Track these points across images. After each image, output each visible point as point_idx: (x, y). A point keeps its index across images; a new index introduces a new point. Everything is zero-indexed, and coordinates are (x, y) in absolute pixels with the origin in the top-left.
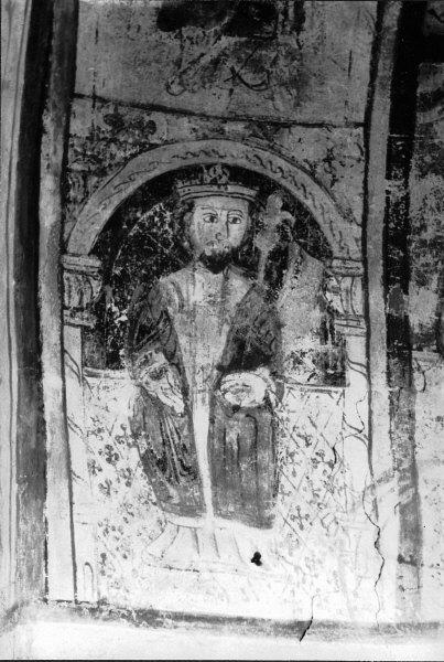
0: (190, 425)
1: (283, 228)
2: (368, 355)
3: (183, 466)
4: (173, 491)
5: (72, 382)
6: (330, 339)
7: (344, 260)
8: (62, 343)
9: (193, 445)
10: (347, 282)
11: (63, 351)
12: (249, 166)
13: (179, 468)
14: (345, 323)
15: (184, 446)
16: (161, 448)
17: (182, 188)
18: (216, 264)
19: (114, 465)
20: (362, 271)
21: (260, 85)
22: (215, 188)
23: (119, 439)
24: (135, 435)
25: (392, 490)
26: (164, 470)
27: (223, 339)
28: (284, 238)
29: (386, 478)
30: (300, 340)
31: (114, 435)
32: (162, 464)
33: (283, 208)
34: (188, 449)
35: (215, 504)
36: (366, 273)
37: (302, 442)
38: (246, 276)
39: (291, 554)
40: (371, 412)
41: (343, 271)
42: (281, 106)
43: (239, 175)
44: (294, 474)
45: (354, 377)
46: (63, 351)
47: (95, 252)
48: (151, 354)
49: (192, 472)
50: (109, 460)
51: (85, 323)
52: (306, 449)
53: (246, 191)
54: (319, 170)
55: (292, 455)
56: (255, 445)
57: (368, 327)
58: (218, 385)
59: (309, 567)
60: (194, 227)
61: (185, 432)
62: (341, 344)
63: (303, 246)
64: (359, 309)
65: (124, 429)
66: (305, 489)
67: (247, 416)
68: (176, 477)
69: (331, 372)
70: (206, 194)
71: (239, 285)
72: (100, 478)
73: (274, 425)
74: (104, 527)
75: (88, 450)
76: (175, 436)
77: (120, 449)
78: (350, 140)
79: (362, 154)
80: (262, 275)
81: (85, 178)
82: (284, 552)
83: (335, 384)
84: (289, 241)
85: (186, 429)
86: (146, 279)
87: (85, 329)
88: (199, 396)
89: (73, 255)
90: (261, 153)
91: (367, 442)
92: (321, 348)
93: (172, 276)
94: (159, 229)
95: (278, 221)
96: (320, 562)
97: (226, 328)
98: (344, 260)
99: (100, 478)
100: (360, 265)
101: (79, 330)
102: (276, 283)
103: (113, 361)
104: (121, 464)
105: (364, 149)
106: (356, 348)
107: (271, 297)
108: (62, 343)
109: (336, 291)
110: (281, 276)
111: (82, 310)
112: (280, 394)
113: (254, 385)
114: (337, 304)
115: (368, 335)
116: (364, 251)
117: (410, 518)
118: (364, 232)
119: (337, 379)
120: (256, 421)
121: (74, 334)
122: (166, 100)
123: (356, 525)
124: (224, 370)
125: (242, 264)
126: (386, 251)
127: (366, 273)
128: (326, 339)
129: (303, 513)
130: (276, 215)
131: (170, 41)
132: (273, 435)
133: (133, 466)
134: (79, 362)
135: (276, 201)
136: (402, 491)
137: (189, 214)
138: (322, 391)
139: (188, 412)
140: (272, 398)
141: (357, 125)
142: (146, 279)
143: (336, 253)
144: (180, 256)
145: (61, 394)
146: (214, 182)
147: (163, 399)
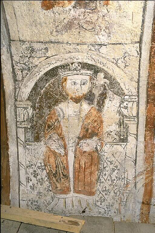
0: (67, 159)
1: (104, 85)
2: (137, 131)
3: (63, 175)
4: (58, 185)
5: (21, 149)
6: (122, 126)
7: (130, 96)
8: (17, 135)
9: (67, 166)
10: (130, 105)
11: (17, 138)
12: (90, 62)
13: (61, 175)
14: (129, 120)
15: (64, 167)
16: (55, 169)
17: (62, 73)
18: (77, 100)
19: (36, 178)
20: (137, 100)
21: (92, 29)
22: (75, 72)
23: (39, 168)
24: (45, 165)
25: (143, 178)
26: (55, 177)
27: (80, 127)
28: (105, 89)
29: (141, 173)
30: (110, 126)
31: (37, 166)
32: (55, 175)
33: (104, 78)
34: (66, 168)
35: (74, 188)
36: (138, 100)
37: (109, 163)
38: (89, 104)
39: (101, 204)
40: (136, 152)
41: (129, 100)
42: (103, 39)
43: (85, 66)
44: (105, 175)
45: (131, 139)
46: (17, 138)
47: (29, 99)
48: (52, 135)
49: (66, 177)
50: (34, 176)
51: (26, 126)
52: (110, 166)
53: (89, 72)
54: (119, 61)
55: (105, 168)
56: (91, 164)
57: (138, 121)
58: (78, 144)
59: (107, 208)
60: (67, 86)
61: (65, 162)
62: (127, 128)
63: (113, 92)
64: (135, 114)
65: (41, 164)
66: (109, 180)
67: (89, 154)
68: (60, 179)
69: (123, 138)
70: (72, 74)
71: (85, 107)
72: (31, 184)
73: (99, 158)
74: (31, 201)
75: (26, 173)
76: (61, 164)
77: (39, 171)
78: (133, 49)
79: (138, 54)
80: (96, 103)
81: (22, 72)
82: (99, 204)
83: (123, 142)
84: (107, 90)
85: (65, 160)
86: (50, 107)
87: (26, 128)
88: (71, 148)
89: (20, 101)
90: (94, 57)
91: (134, 162)
92: (118, 130)
93: (60, 105)
94: (53, 89)
95: (102, 83)
96: (112, 206)
97: (81, 124)
98: (130, 96)
99: (31, 184)
100: (136, 97)
101: (23, 129)
102: (101, 104)
103: (37, 139)
104: (39, 177)
105: (139, 52)
106: (132, 129)
107: (100, 110)
108: (17, 135)
109: (126, 108)
110: (103, 102)
111: (24, 121)
112: (102, 146)
113: (89, 145)
114: (125, 112)
115: (138, 124)
116: (138, 92)
117: (149, 188)
118: (138, 85)
119: (124, 140)
120: (92, 157)
121: (21, 131)
122: (53, 39)
123: (127, 192)
124: (80, 139)
125: (88, 99)
126: (148, 91)
127: (138, 100)
128: (121, 125)
129: (107, 188)
130: (101, 79)
131: (49, 13)
132: (98, 161)
133: (44, 177)
134: (24, 141)
135: (101, 75)
136: (146, 179)
137: (65, 82)
138: (118, 145)
139: (66, 154)
140: (99, 148)
141: (136, 43)
142: (50, 107)
143: (126, 92)
144: (64, 97)
145: (17, 154)
146: (75, 69)
147: (56, 151)
